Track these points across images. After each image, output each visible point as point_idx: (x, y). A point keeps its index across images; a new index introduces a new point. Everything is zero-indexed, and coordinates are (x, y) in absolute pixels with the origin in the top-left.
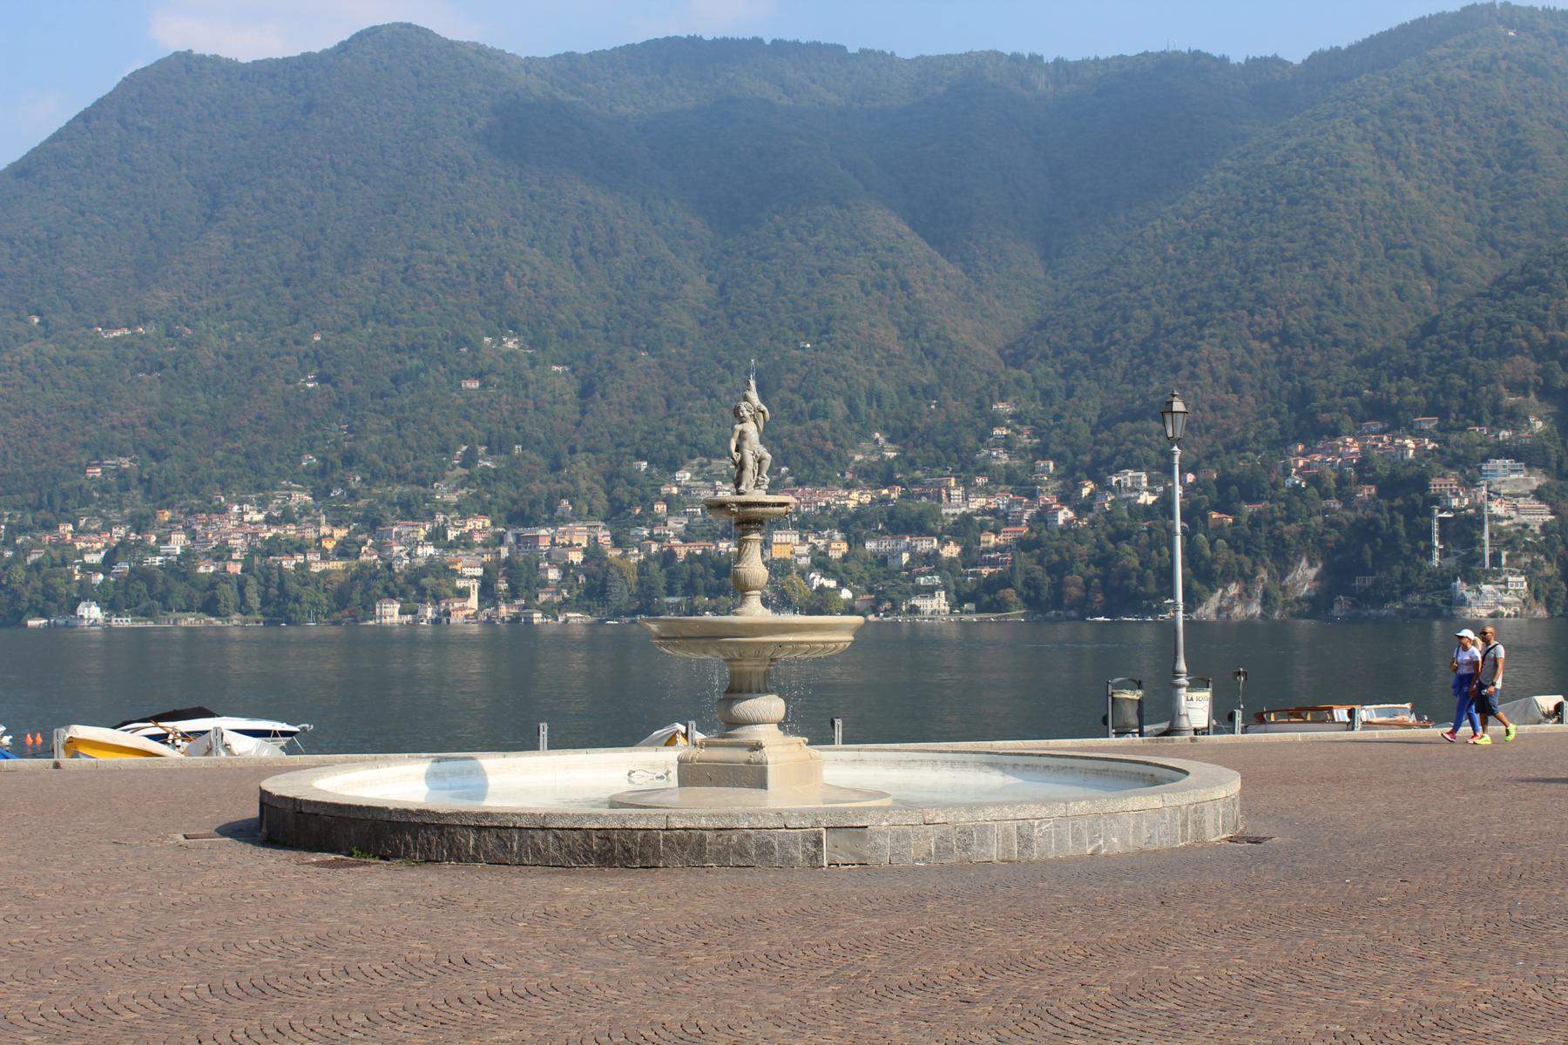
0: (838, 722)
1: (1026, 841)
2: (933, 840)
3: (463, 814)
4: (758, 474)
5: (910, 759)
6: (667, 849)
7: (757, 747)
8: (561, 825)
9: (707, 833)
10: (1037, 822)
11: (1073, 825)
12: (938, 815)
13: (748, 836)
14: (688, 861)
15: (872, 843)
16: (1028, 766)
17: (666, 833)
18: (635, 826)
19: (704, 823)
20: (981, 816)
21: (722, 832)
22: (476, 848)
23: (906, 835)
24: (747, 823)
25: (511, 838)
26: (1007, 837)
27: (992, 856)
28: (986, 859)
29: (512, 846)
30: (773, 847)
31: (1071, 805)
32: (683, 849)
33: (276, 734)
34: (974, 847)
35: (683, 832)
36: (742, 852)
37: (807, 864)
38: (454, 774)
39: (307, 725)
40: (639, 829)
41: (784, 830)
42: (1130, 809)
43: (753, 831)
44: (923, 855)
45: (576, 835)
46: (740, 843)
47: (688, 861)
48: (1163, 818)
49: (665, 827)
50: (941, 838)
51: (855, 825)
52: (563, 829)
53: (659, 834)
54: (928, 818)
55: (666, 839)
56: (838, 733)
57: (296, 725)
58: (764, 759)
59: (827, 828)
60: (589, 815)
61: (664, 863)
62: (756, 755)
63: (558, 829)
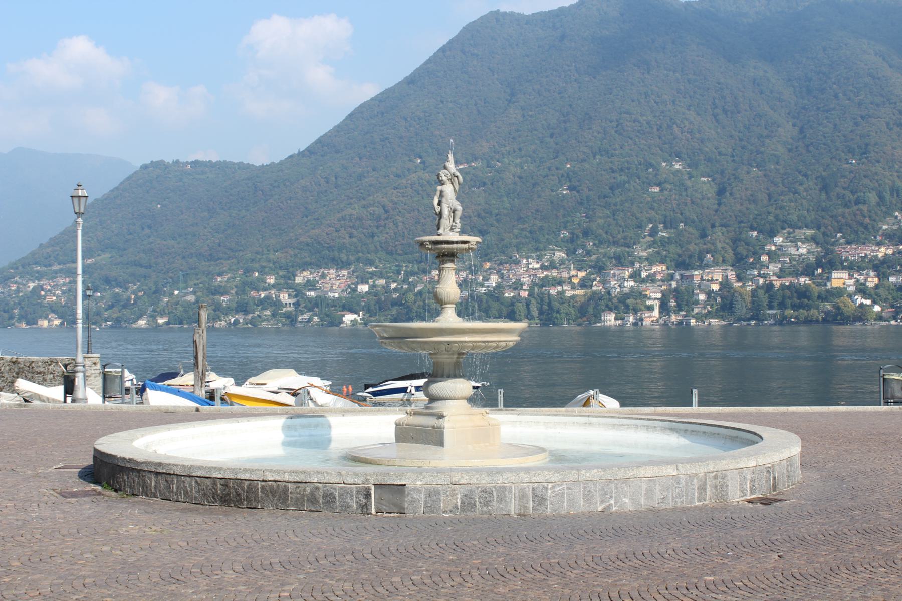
0: (695, 392)
1: (540, 500)
2: (459, 496)
4: (453, 221)
5: (621, 424)
6: (263, 495)
7: (441, 417)
8: (199, 474)
9: (289, 485)
10: (550, 486)
11: (585, 488)
12: (463, 477)
13: (317, 488)
14: (277, 505)
15: (409, 498)
16: (693, 431)
17: (263, 483)
18: (243, 477)
19: (287, 477)
20: (500, 480)
21: (299, 485)
22: (156, 487)
23: (437, 493)
24: (316, 479)
25: (172, 482)
26: (523, 496)
27: (509, 511)
28: (504, 513)
30: (335, 498)
31: (583, 472)
34: (494, 503)
35: (273, 483)
36: (313, 500)
37: (359, 511)
38: (303, 426)
39: (485, 383)
40: (246, 480)
41: (343, 485)
42: (641, 476)
43: (320, 485)
44: (450, 508)
45: (208, 482)
46: (312, 494)
47: (277, 505)
48: (678, 483)
49: (261, 480)
50: (466, 495)
51: (395, 483)
52: (200, 477)
53: (258, 484)
54: (454, 480)
55: (263, 488)
56: (695, 399)
58: (442, 426)
59: (374, 485)
60: (215, 468)
61: (261, 506)
63: (197, 477)
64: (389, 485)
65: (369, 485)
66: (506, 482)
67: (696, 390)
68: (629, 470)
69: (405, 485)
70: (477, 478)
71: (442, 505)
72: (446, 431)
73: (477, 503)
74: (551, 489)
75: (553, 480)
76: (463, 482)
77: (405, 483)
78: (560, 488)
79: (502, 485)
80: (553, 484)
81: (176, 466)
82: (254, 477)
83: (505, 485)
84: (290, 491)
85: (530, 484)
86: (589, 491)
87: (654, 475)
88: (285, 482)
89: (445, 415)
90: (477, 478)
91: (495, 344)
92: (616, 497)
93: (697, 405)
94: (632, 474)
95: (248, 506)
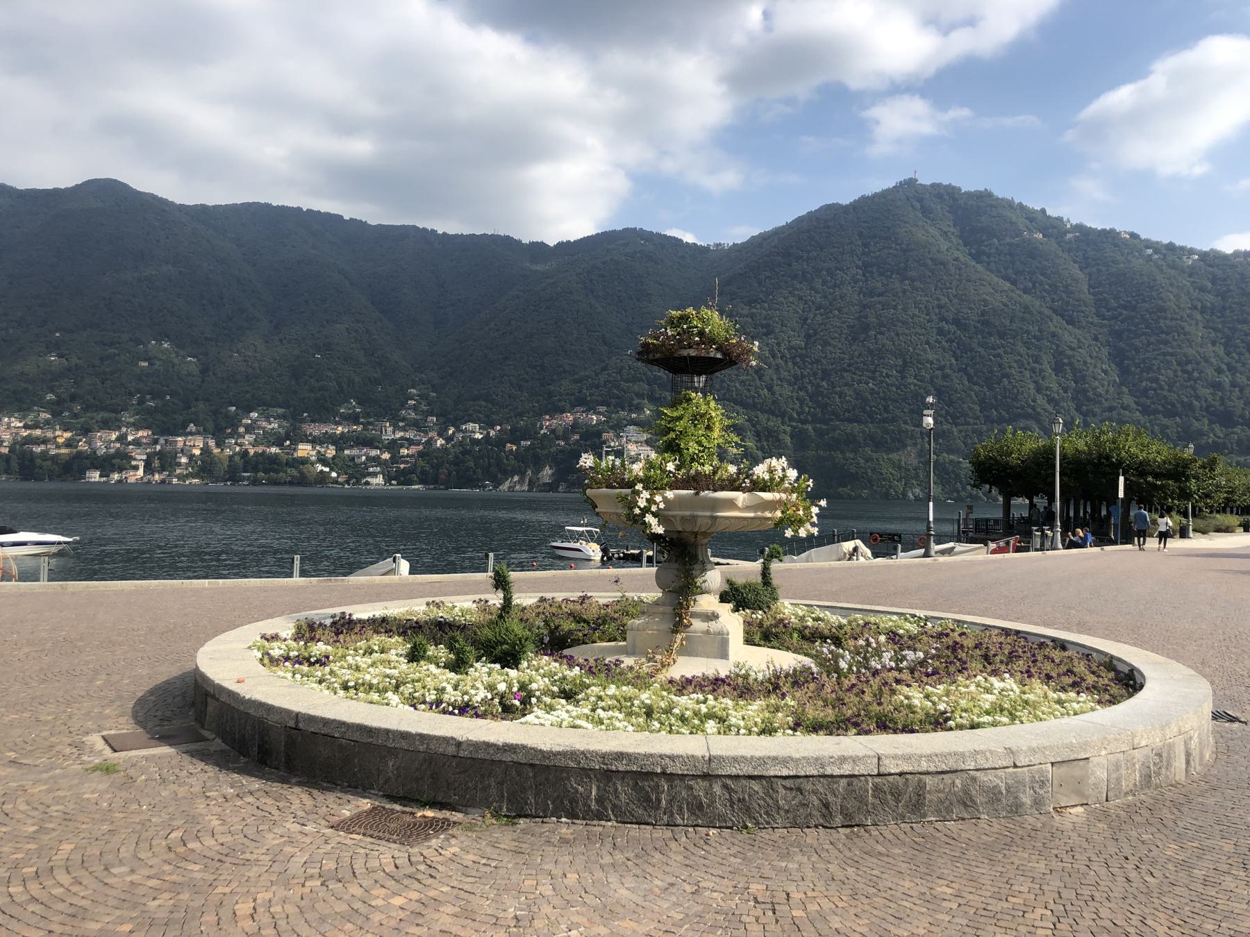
3: (583, 753)
8: (734, 771)
9: (927, 779)
17: (877, 780)
18: (837, 772)
22: (600, 801)
29: (659, 801)
32: (898, 801)
36: (966, 801)
40: (842, 776)
41: (1011, 770)
45: (756, 786)
46: (966, 791)
52: (737, 777)
55: (876, 788)
58: (725, 631)
60: (775, 758)
62: (713, 626)
63: (730, 777)
71: (1123, 784)
81: (669, 757)
82: (860, 769)
84: (928, 788)
88: (920, 773)
95: (846, 823)
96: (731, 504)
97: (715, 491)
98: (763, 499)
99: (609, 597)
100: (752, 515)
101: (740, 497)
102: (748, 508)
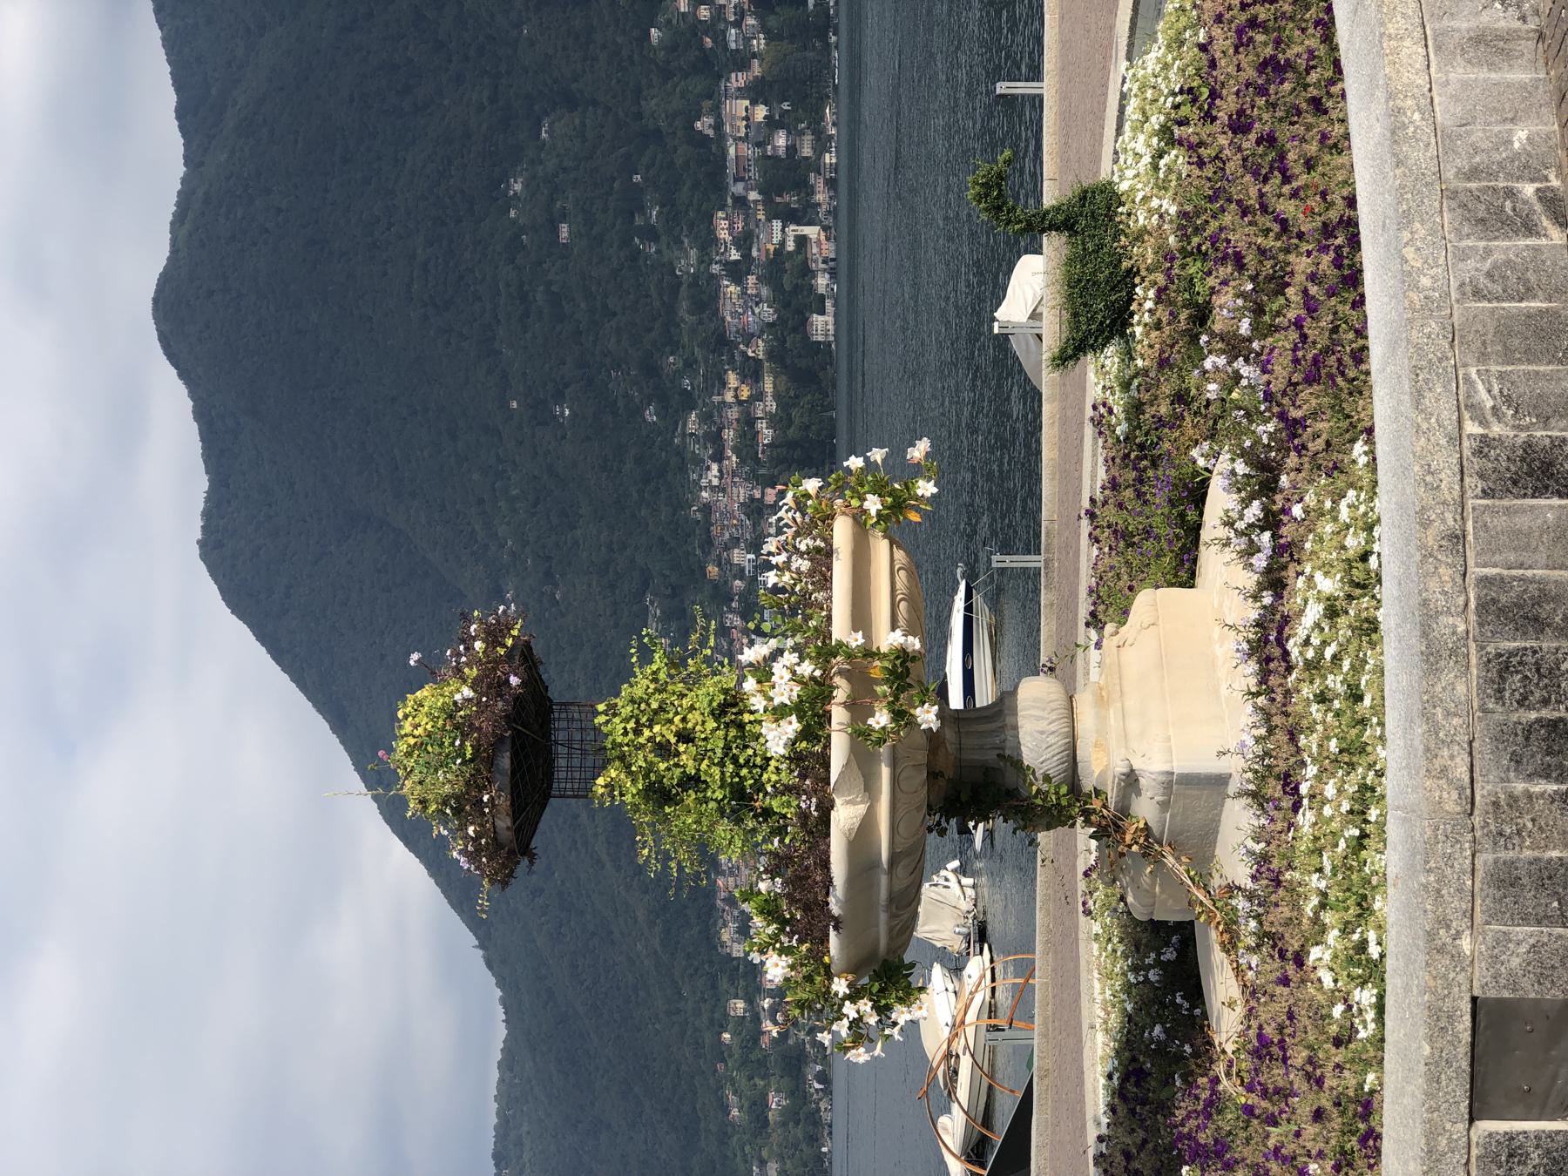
0: (1002, 88)
2: (1519, 787)
33: (968, 608)
42: (1422, 80)
50: (1516, 760)
51: (1466, 1037)
56: (1022, 88)
57: (958, 583)
58: (1163, 778)
59: (1471, 1121)
64: (1472, 1065)
65: (1474, 1139)
66: (1461, 601)
67: (998, 85)
68: (1404, 126)
69: (1474, 1000)
70: (1448, 714)
71: (1555, 854)
72: (1182, 766)
73: (1546, 713)
74: (1483, 423)
75: (1448, 417)
76: (1462, 772)
77: (1467, 998)
78: (1480, 387)
79: (1473, 617)
80: (1466, 415)
83: (1472, 604)
85: (1470, 503)
86: (1489, 275)
87: (1418, 34)
89: (1125, 770)
90: (1448, 714)
91: (903, 606)
92: (1510, 176)
93: (1035, 84)
94: (1417, 116)
96: (862, 837)
97: (828, 883)
98: (846, 766)
99: (1094, 455)
100: (885, 772)
101: (844, 816)
102: (870, 789)
